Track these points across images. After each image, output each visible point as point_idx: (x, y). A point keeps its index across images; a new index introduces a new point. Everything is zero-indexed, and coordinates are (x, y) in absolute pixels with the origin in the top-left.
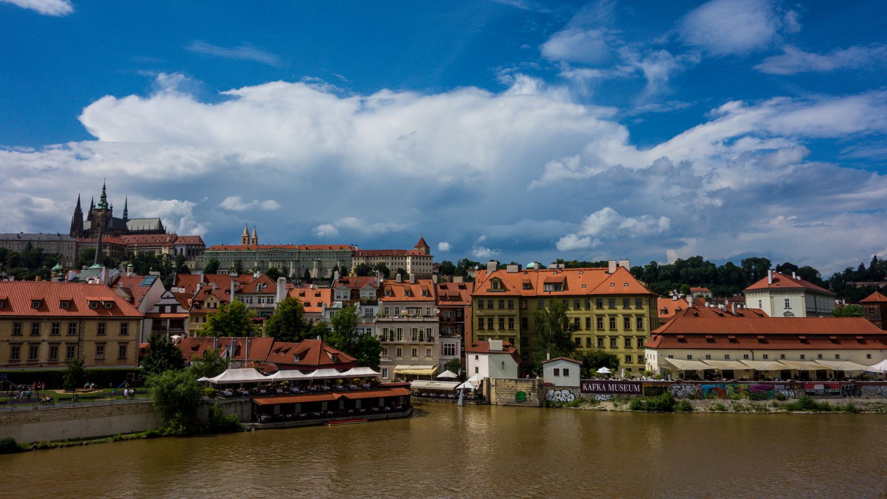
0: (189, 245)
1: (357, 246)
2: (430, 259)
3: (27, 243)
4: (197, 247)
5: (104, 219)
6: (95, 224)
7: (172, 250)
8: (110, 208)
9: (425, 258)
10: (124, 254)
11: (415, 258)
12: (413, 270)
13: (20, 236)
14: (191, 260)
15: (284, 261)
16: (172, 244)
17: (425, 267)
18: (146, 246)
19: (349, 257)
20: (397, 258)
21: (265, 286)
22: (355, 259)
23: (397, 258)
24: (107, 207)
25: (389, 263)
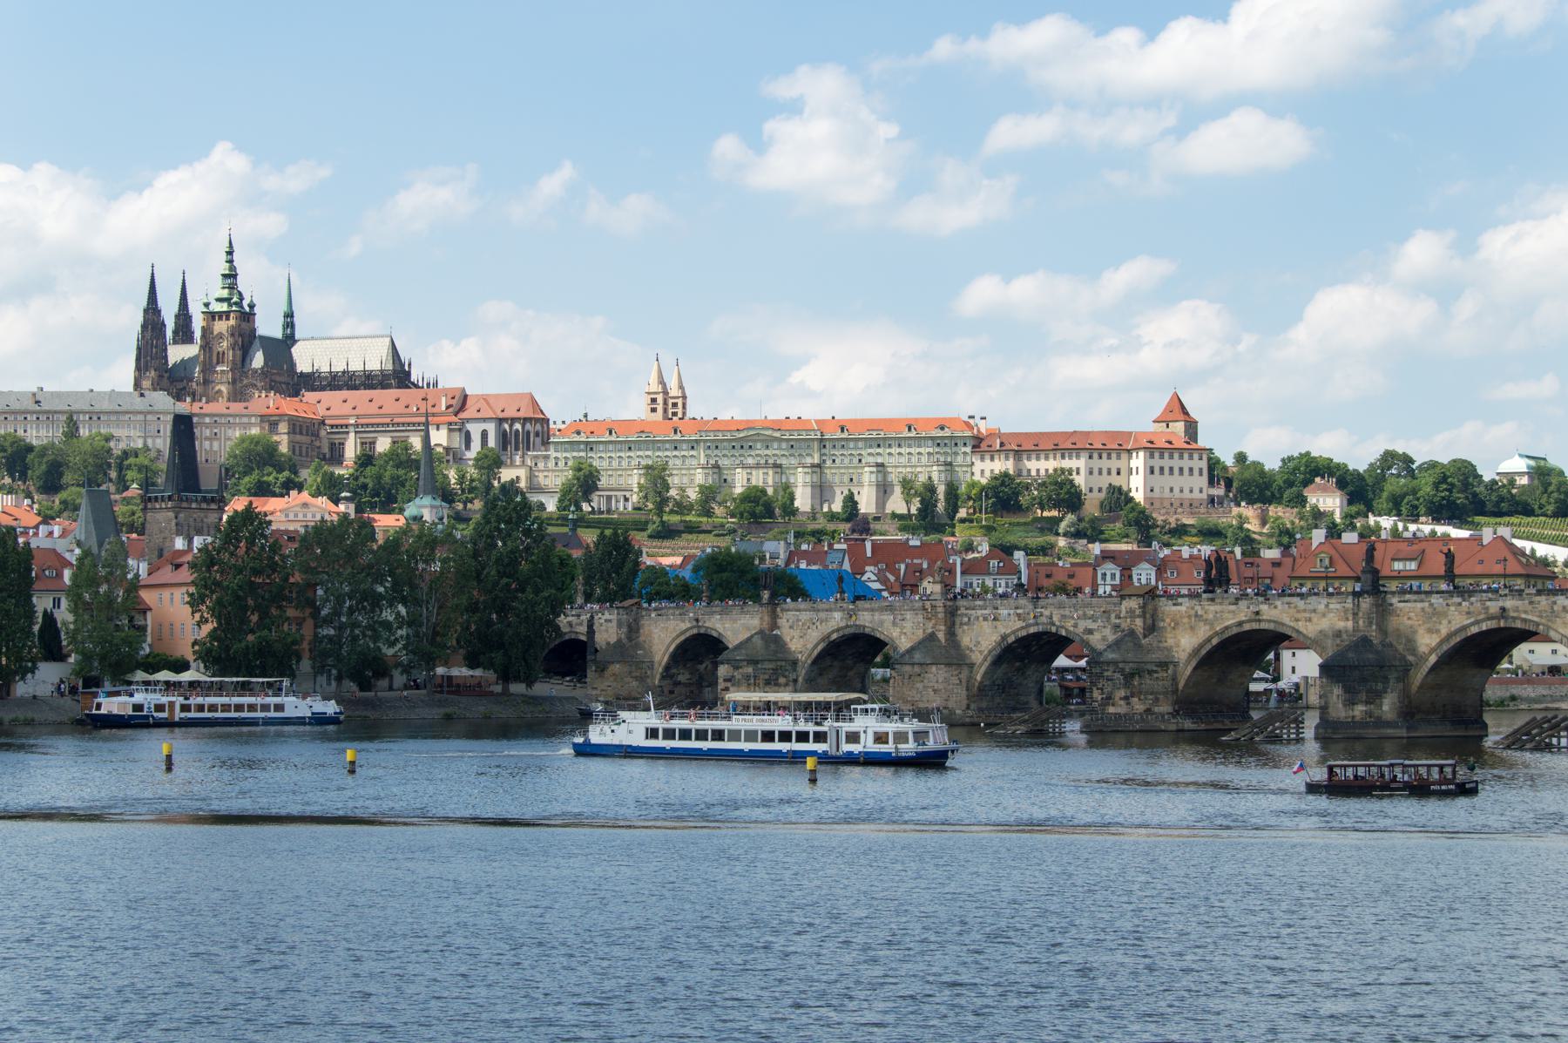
0: (505, 420)
1: (982, 418)
2: (1201, 459)
3: (64, 418)
4: (528, 426)
5: (236, 343)
6: (210, 358)
7: (457, 435)
8: (247, 309)
9: (1186, 456)
10: (319, 447)
11: (1157, 455)
12: (1152, 491)
13: (38, 398)
14: (512, 465)
15: (776, 466)
16: (454, 419)
17: (1186, 481)
18: (383, 425)
19: (965, 453)
20: (1104, 455)
21: (1001, 564)
22: (982, 459)
23: (1104, 455)
24: (242, 307)
25: (1082, 471)
